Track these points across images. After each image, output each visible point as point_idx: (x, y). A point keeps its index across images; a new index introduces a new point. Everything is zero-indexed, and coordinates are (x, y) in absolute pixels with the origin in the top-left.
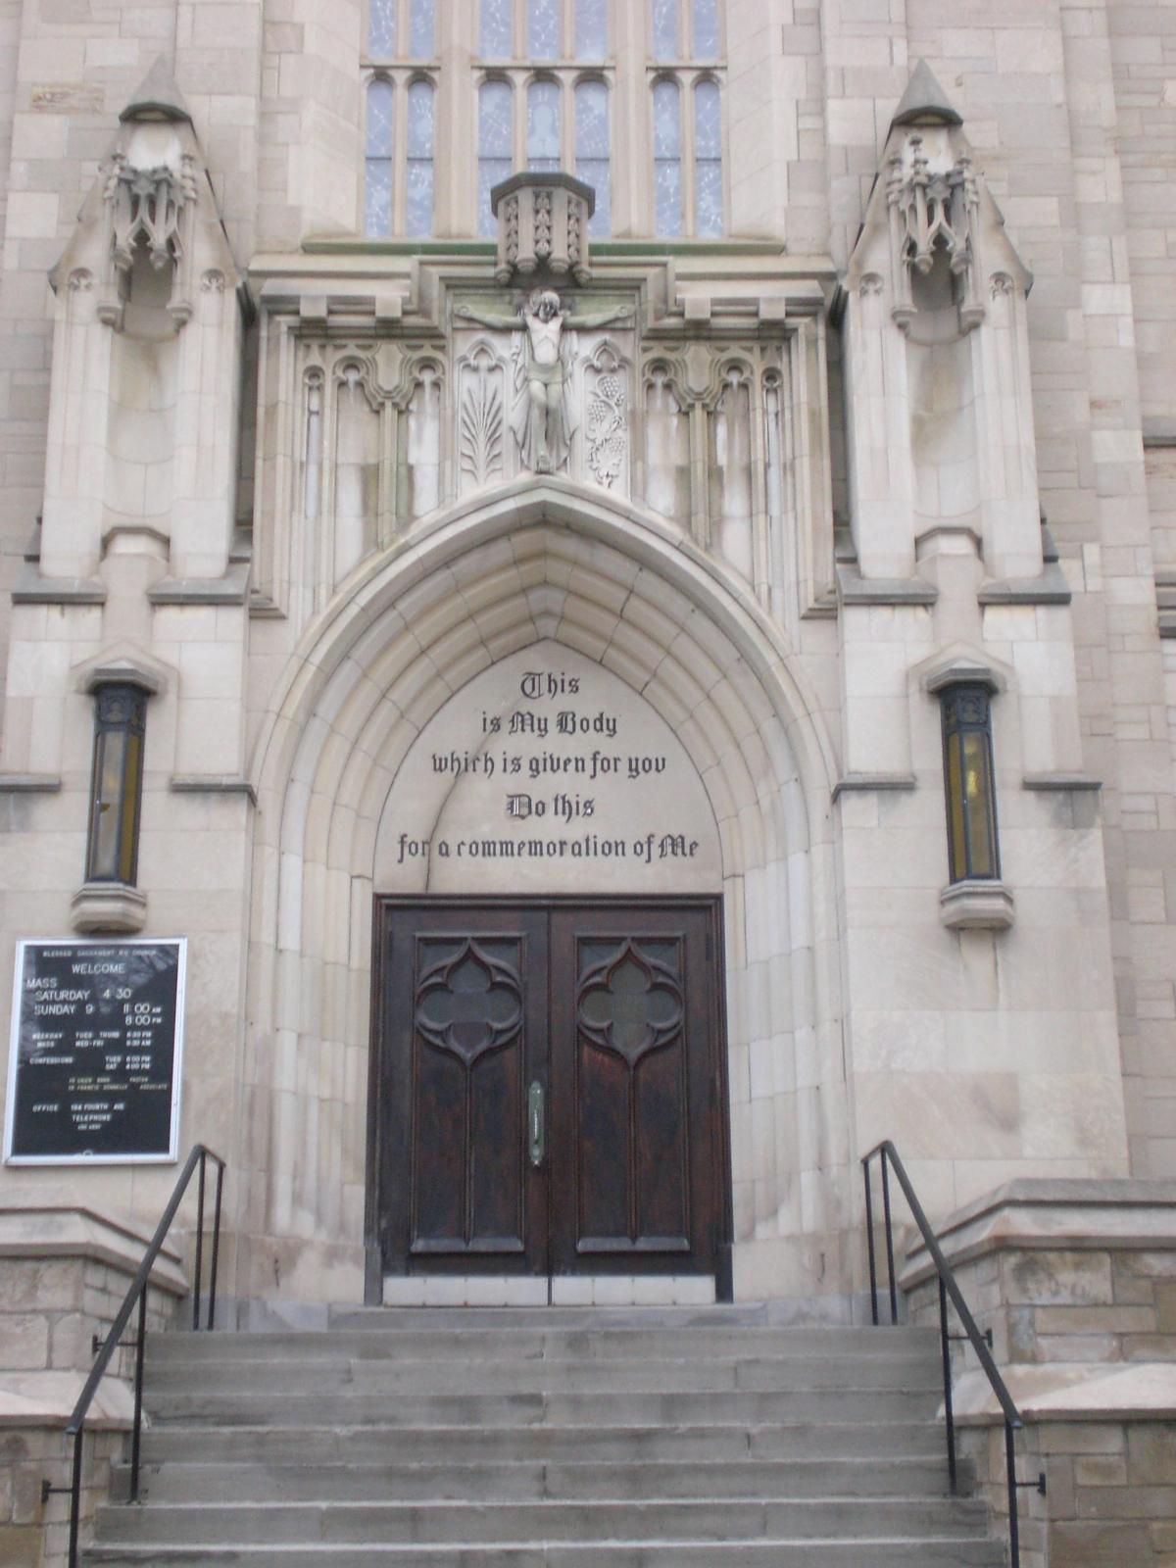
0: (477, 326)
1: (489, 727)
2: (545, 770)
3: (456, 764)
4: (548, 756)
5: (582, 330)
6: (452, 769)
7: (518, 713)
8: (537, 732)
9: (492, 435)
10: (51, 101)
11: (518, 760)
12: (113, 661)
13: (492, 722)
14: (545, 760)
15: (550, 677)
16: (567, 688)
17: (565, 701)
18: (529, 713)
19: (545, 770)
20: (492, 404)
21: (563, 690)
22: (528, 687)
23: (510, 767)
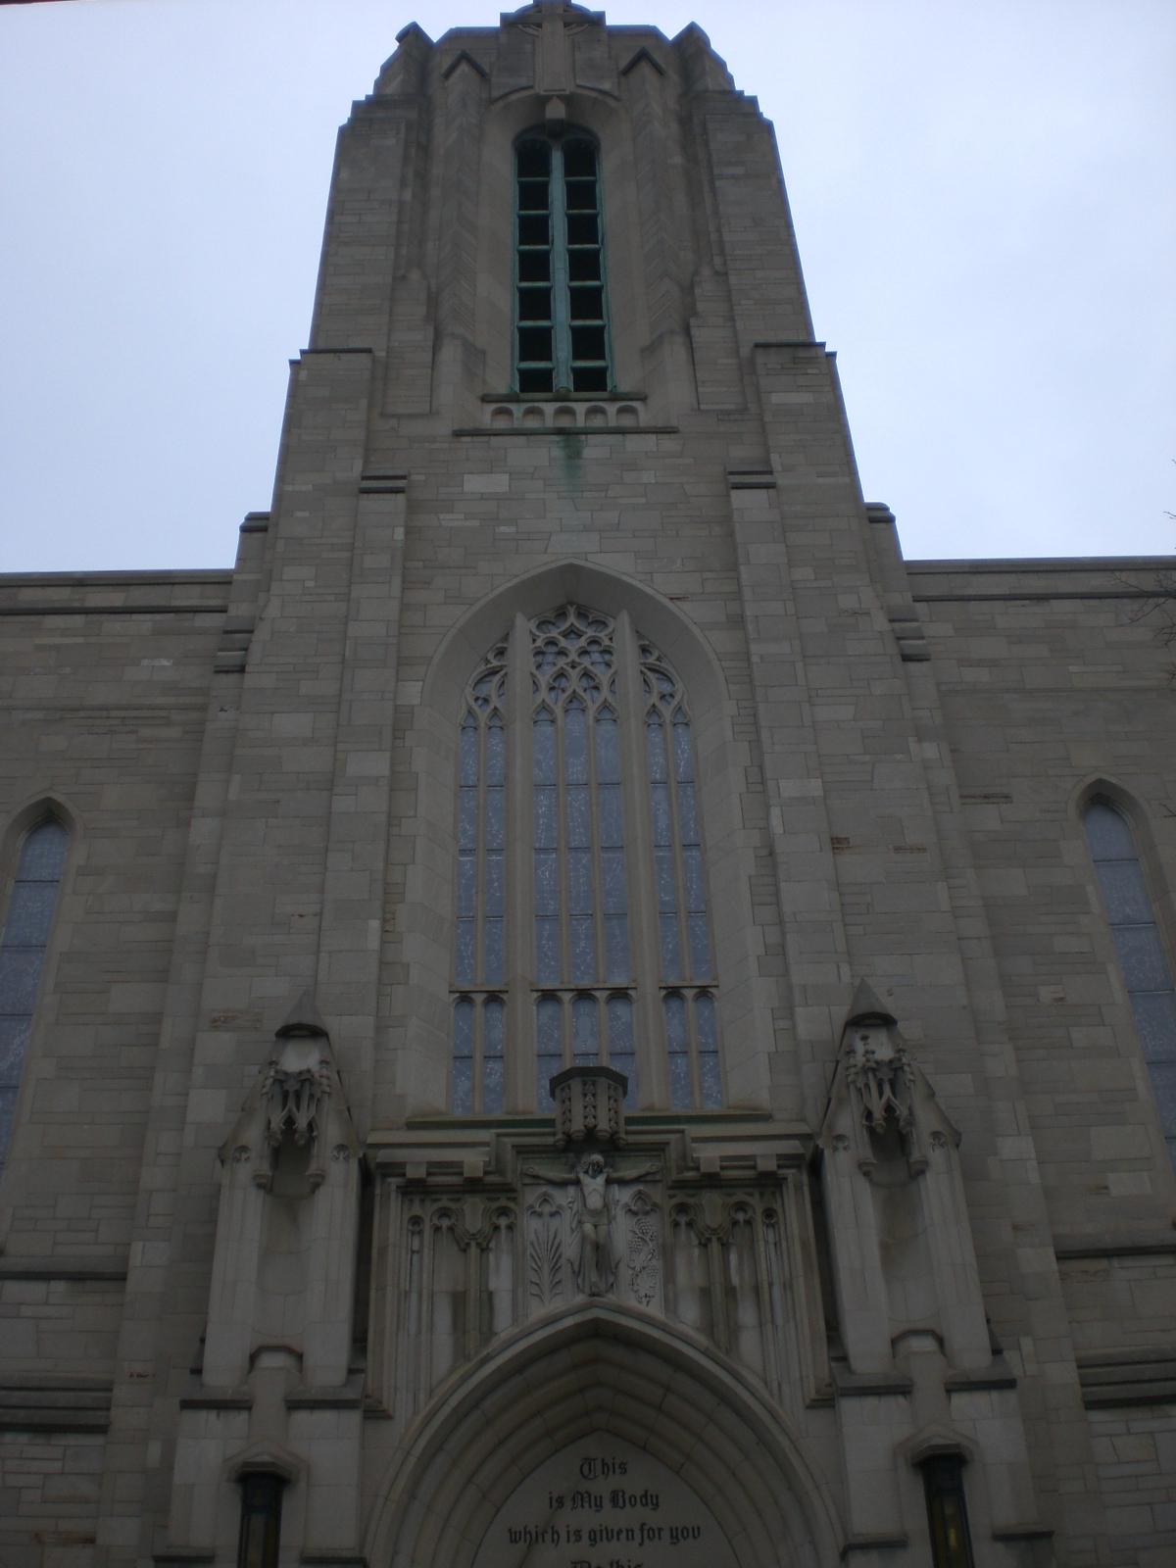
0: (542, 1182)
1: (555, 1504)
4: (603, 1528)
5: (623, 1182)
6: (525, 1541)
7: (578, 1492)
8: (594, 1508)
9: (554, 1267)
11: (579, 1531)
13: (557, 1501)
14: (601, 1531)
15: (603, 1460)
18: (587, 1492)
20: (553, 1243)
21: (614, 1472)
22: (586, 1469)
23: (572, 1538)
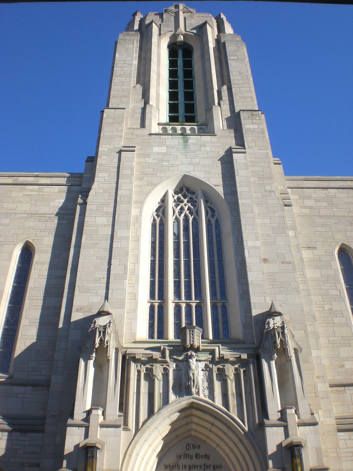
0: (176, 360)
1: (178, 457)
2: (192, 468)
3: (170, 467)
4: (193, 465)
5: (200, 361)
6: (169, 468)
7: (185, 454)
9: (179, 386)
10: (80, 310)
11: (186, 466)
12: (90, 441)
13: (179, 456)
15: (193, 444)
16: (197, 447)
17: (197, 451)
18: (188, 454)
19: (192, 468)
21: (196, 448)
22: (188, 447)
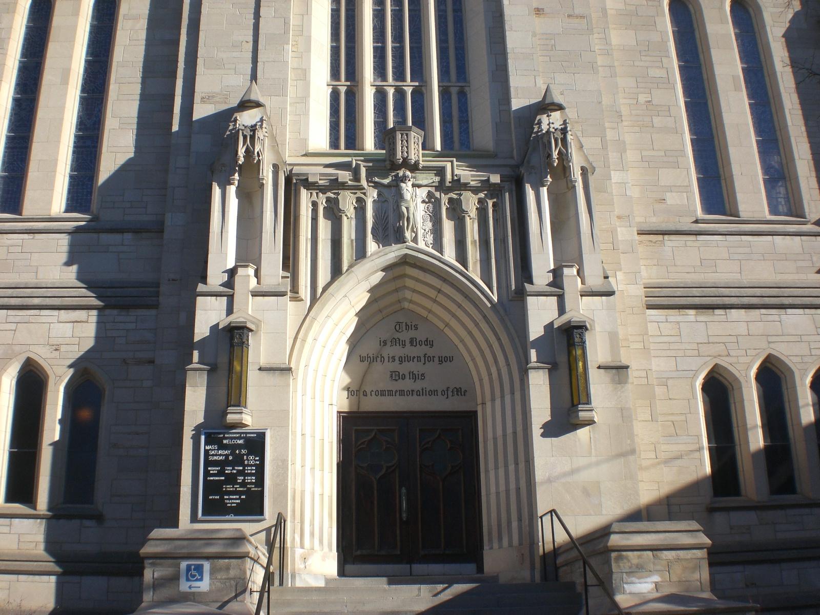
0: (379, 185)
1: (382, 344)
2: (405, 361)
3: (369, 359)
4: (406, 356)
5: (419, 186)
6: (368, 361)
7: (394, 338)
8: (401, 346)
12: (236, 319)
14: (405, 357)
15: (406, 323)
16: (413, 328)
17: (412, 334)
18: (398, 338)
19: (405, 361)
20: (384, 215)
21: (411, 329)
22: (397, 327)
23: (391, 360)
